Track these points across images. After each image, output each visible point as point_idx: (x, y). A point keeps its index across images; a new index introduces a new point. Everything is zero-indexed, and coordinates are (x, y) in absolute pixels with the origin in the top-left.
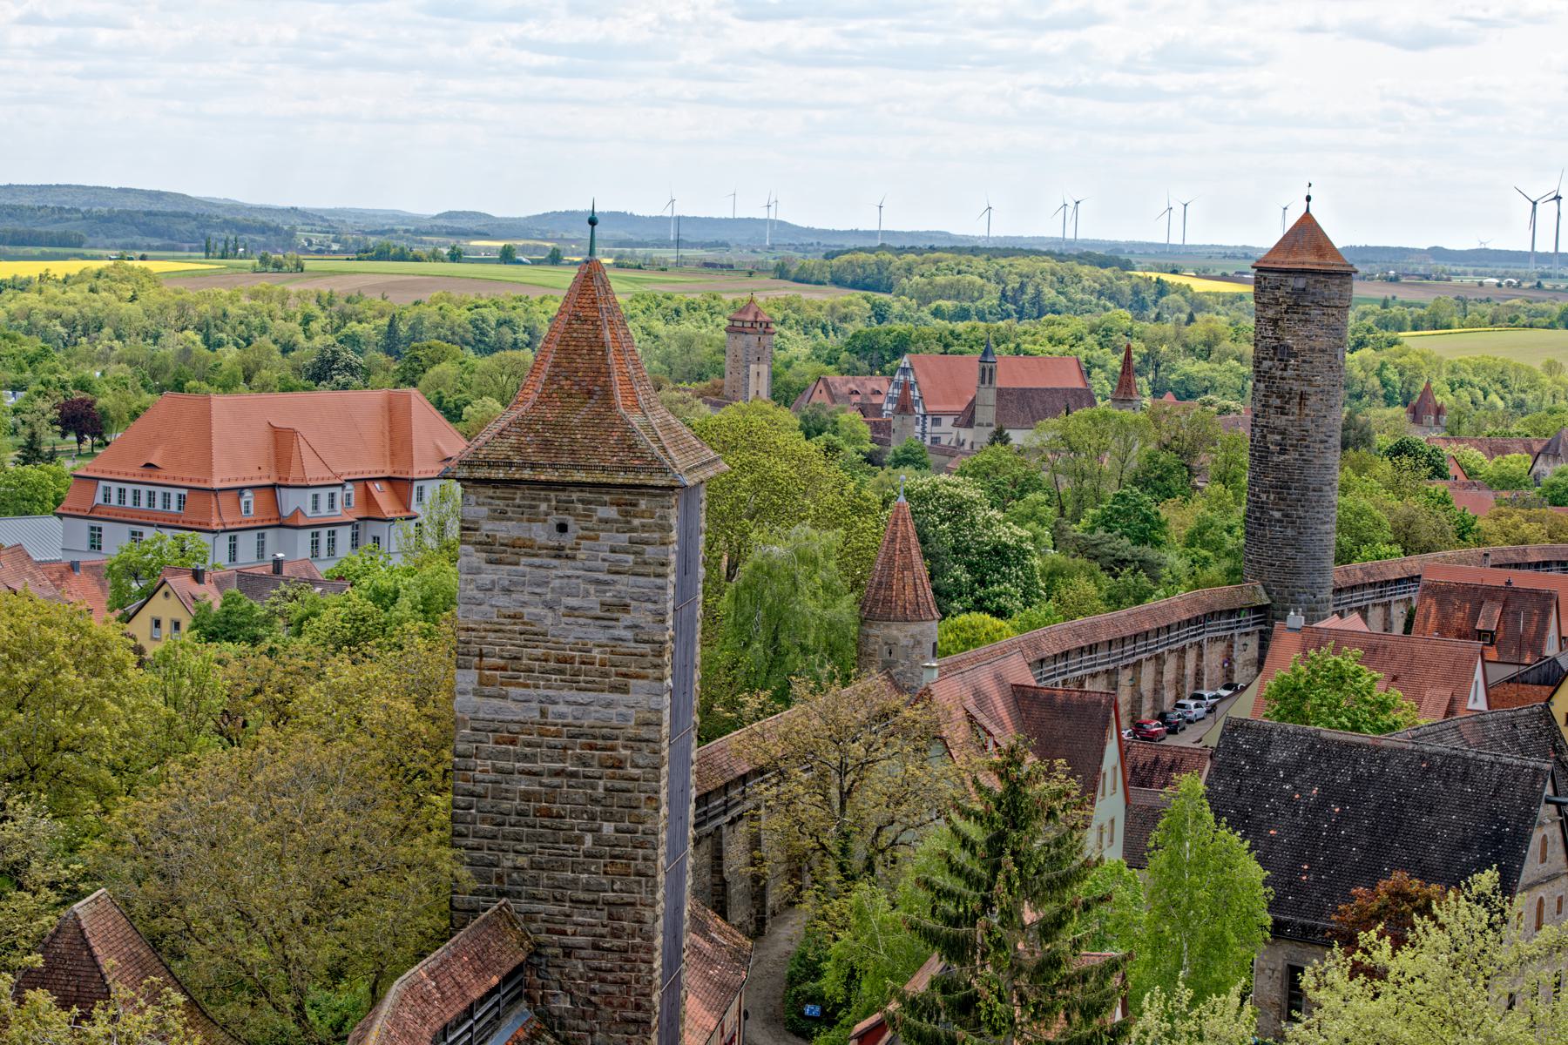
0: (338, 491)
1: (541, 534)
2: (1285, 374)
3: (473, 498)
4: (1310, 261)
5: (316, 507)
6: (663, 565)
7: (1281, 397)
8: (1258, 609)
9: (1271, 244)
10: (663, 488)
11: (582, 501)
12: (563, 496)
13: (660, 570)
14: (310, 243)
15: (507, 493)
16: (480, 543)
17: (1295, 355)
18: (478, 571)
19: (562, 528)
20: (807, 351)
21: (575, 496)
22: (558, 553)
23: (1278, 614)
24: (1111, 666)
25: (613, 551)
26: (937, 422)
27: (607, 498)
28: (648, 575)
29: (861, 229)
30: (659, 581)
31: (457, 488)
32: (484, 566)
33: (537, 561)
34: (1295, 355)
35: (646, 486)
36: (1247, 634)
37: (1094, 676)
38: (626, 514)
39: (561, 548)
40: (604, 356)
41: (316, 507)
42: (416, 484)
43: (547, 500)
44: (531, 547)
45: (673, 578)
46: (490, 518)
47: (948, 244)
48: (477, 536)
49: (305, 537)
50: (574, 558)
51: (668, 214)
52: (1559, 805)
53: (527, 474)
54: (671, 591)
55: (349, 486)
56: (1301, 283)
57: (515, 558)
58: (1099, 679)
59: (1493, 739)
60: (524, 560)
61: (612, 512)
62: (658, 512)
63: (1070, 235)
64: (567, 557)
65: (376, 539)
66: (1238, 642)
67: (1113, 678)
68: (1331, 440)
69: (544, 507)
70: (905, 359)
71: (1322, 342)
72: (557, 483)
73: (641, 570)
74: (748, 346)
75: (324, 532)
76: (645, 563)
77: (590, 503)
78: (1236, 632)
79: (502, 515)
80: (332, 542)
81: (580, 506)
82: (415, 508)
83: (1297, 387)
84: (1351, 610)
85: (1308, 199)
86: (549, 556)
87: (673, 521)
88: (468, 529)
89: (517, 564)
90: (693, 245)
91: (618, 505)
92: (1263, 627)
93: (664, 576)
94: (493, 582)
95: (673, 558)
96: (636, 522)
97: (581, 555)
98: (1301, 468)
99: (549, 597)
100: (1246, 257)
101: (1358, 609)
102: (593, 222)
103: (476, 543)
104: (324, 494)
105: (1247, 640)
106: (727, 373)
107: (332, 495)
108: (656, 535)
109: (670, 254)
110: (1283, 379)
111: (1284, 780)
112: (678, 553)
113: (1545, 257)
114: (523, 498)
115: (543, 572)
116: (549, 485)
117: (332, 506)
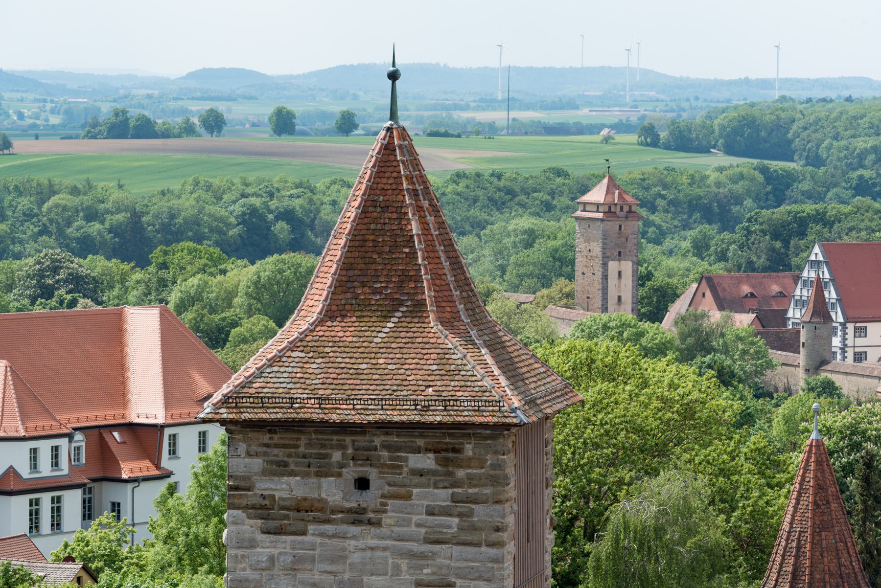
0: (63, 443)
1: (333, 491)
3: (242, 448)
5: (34, 466)
6: (498, 530)
10: (496, 426)
11: (387, 447)
12: (362, 440)
13: (494, 537)
14: (21, 116)
15: (287, 437)
16: (253, 507)
18: (252, 544)
19: (362, 484)
20: (686, 244)
21: (377, 441)
22: (358, 517)
25: (430, 512)
26: (861, 332)
27: (420, 442)
28: (478, 545)
29: (753, 77)
30: (493, 551)
31: (217, 434)
32: (260, 537)
33: (329, 528)
35: (473, 425)
38: (445, 462)
39: (364, 511)
40: (413, 255)
41: (34, 466)
42: (168, 432)
43: (343, 447)
44: (321, 510)
45: (511, 547)
46: (265, 473)
47: (868, 94)
48: (252, 498)
49: (20, 505)
50: (378, 524)
51: (494, 63)
53: (316, 415)
54: (509, 564)
55: (79, 436)
57: (300, 526)
60: (311, 528)
61: (428, 461)
62: (490, 459)
64: (370, 523)
65: (116, 507)
69: (337, 456)
70: (817, 249)
72: (354, 425)
73: (469, 538)
74: (605, 237)
75: (46, 499)
76: (474, 528)
77: (399, 449)
79: (279, 468)
80: (57, 512)
81: (385, 454)
82: (166, 462)
86: (343, 521)
87: (510, 471)
88: (236, 488)
89: (304, 533)
90: (527, 107)
91: (436, 451)
93: (499, 544)
94: (272, 559)
95: (511, 520)
96: (461, 473)
97: (388, 519)
99: (346, 576)
102: (394, 76)
103: (245, 508)
104: (45, 448)
106: (578, 274)
107: (56, 449)
108: (487, 491)
109: (499, 116)
112: (518, 515)
114: (309, 445)
115: (335, 542)
116: (344, 428)
117: (56, 464)
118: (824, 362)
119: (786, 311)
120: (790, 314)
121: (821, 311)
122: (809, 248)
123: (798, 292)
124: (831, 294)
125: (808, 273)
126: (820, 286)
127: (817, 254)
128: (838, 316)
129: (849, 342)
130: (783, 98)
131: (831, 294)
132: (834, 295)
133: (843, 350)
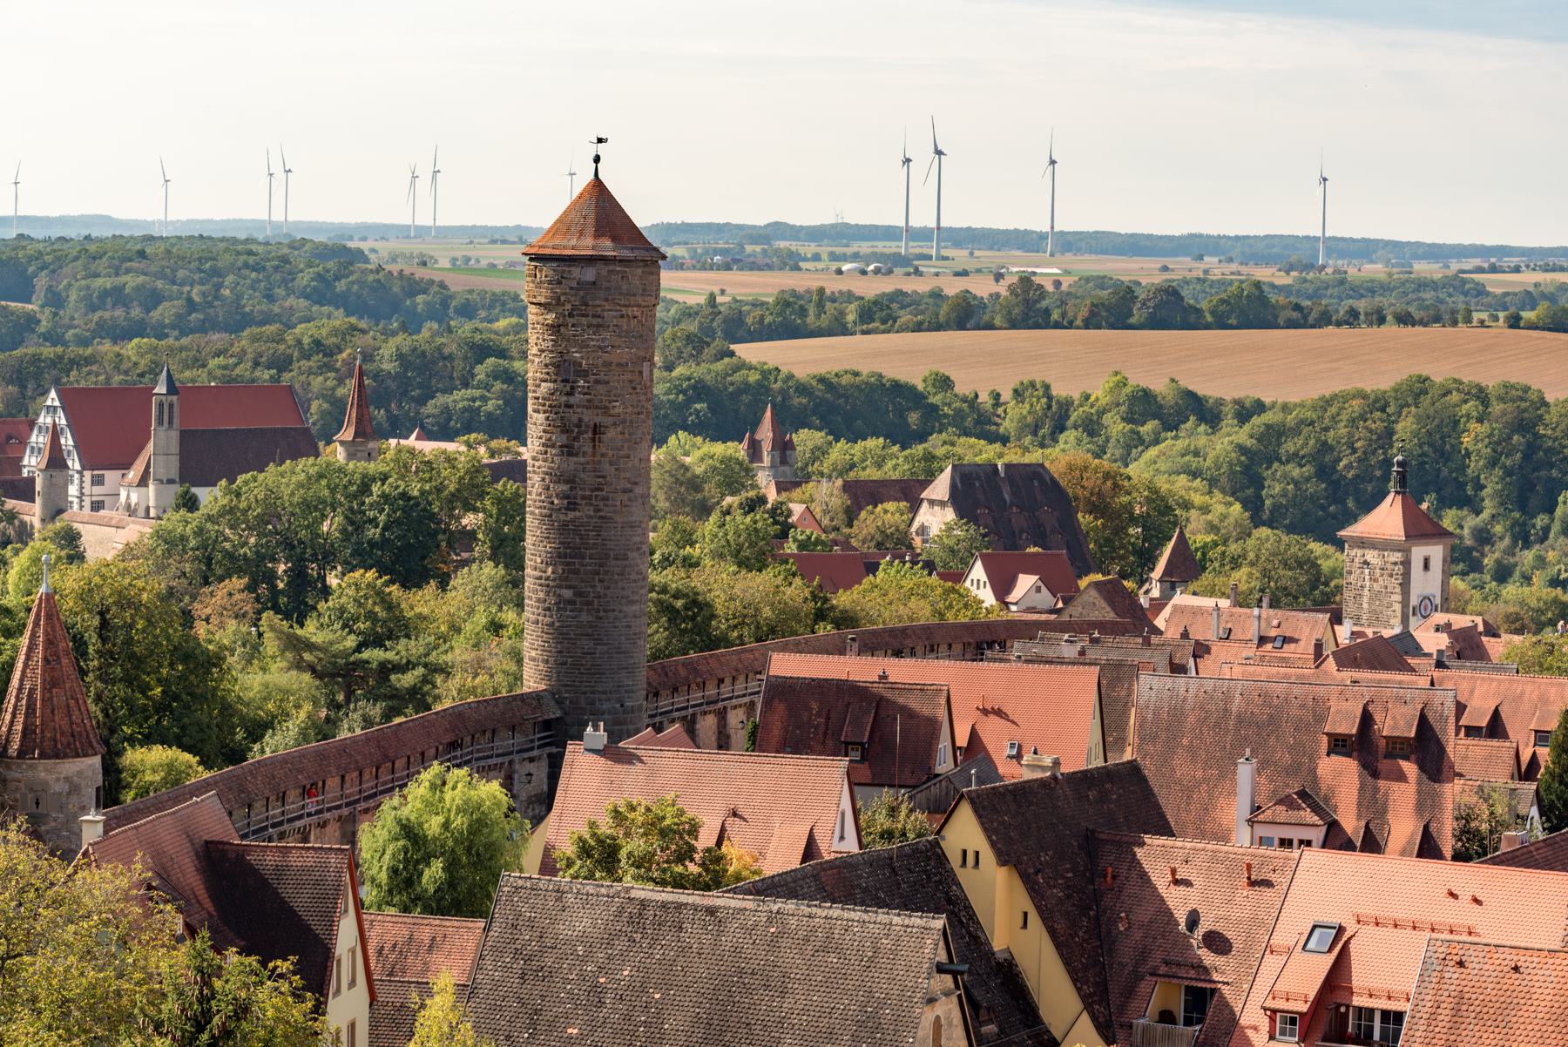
2: (572, 400)
4: (607, 247)
7: (565, 430)
8: (547, 725)
9: (547, 224)
17: (584, 374)
23: (573, 730)
24: (345, 811)
34: (584, 374)
36: (532, 760)
37: (323, 825)
52: (955, 974)
56: (589, 274)
58: (329, 829)
59: (865, 890)
63: (278, 216)
66: (522, 769)
67: (349, 828)
68: (638, 490)
70: (53, 394)
71: (623, 354)
78: (516, 757)
83: (589, 417)
84: (673, 721)
85: (597, 159)
92: (554, 750)
98: (598, 529)
100: (521, 241)
101: (684, 718)
105: (531, 767)
110: (569, 406)
111: (584, 960)
113: (922, 234)
118: (60, 511)
119: (21, 459)
120: (25, 462)
121: (56, 461)
122: (46, 392)
123: (33, 438)
124: (67, 441)
125: (44, 419)
126: (56, 434)
127: (53, 398)
128: (74, 463)
129: (86, 491)
130: (21, 236)
131: (67, 441)
132: (71, 442)
133: (81, 498)
